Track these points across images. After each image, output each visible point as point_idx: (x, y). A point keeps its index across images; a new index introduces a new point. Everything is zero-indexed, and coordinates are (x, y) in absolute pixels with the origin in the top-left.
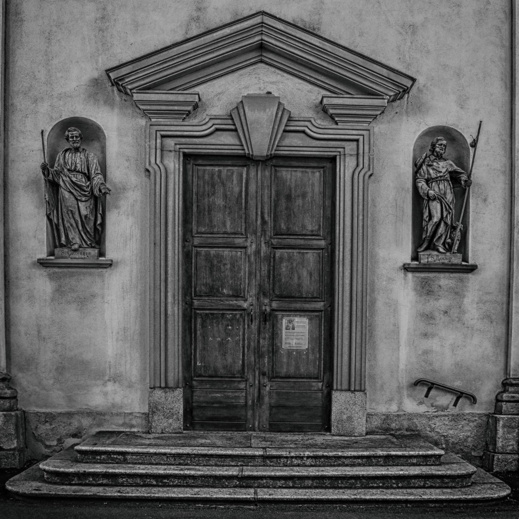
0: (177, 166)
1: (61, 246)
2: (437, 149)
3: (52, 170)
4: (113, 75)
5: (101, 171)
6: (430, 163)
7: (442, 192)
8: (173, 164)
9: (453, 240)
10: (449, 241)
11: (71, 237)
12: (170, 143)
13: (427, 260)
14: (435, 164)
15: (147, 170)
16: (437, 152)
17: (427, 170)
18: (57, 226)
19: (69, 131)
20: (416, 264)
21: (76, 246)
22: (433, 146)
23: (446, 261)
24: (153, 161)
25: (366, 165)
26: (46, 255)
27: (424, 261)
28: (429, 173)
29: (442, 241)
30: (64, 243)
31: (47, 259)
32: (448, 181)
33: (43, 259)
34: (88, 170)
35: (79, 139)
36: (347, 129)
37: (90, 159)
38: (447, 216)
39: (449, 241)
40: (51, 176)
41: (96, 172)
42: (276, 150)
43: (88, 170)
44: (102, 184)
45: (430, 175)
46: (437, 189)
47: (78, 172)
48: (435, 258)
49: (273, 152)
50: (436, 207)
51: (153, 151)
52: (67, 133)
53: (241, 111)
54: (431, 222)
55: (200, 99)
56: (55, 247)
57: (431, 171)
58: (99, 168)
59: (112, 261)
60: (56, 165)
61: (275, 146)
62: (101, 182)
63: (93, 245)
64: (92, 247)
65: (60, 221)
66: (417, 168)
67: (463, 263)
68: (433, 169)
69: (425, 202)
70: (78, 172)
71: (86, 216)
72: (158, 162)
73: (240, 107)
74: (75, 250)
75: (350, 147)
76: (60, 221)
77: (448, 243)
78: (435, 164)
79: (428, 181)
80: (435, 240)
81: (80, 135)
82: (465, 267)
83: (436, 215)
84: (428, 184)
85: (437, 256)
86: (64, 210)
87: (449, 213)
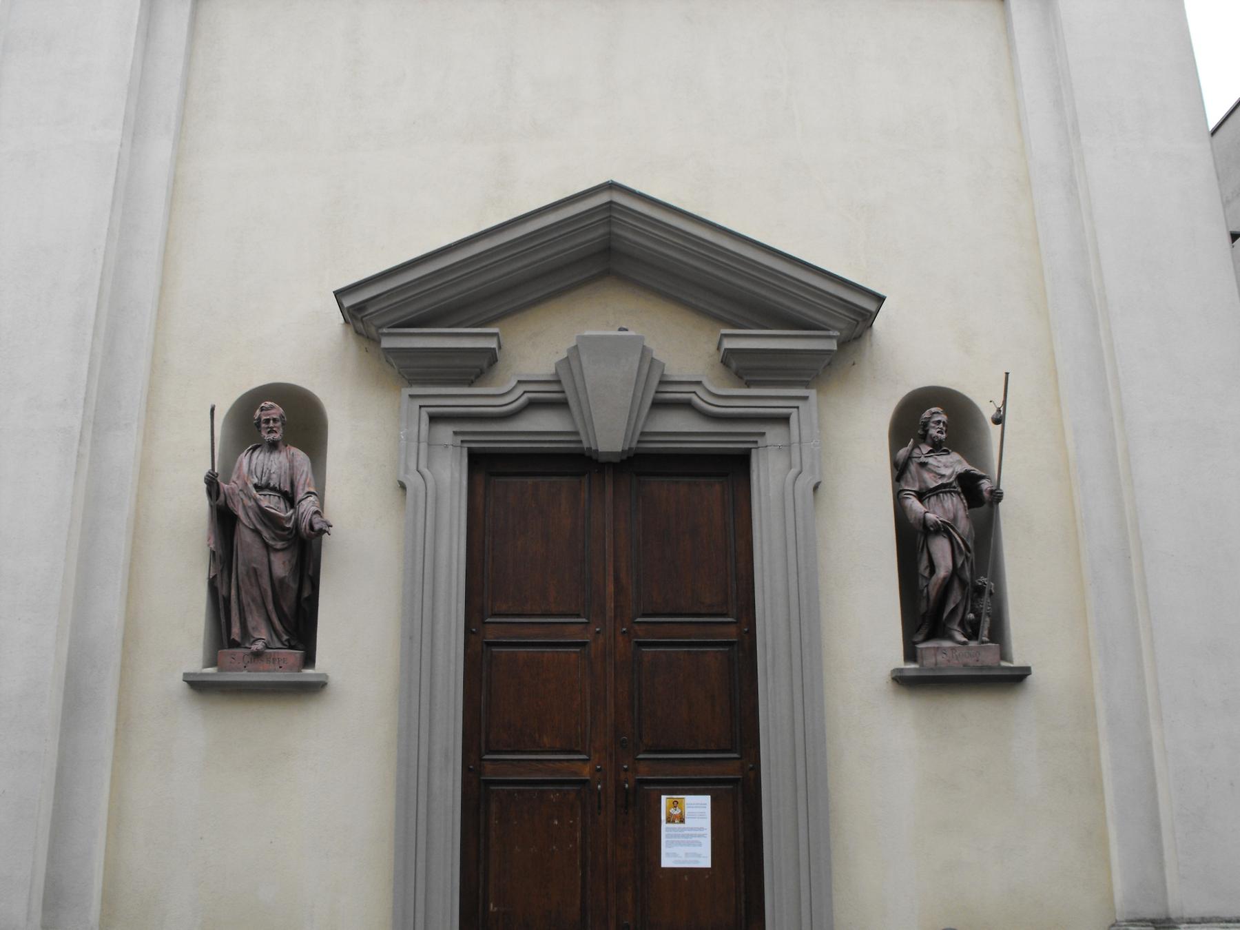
0: (457, 475)
1: (234, 644)
2: (933, 432)
3: (226, 486)
4: (349, 302)
5: (316, 488)
6: (923, 459)
7: (951, 516)
8: (451, 474)
9: (978, 615)
10: (972, 616)
11: (251, 623)
12: (445, 433)
13: (933, 660)
14: (930, 460)
15: (403, 487)
16: (933, 438)
17: (918, 473)
18: (227, 601)
19: (262, 409)
20: (915, 669)
21: (259, 646)
22: (925, 425)
23: (971, 662)
24: (413, 466)
25: (806, 467)
26: (201, 664)
27: (929, 661)
28: (922, 480)
29: (958, 619)
30: (237, 639)
31: (202, 674)
32: (959, 494)
33: (194, 674)
34: (292, 484)
35: (279, 424)
36: (765, 399)
37: (296, 464)
38: (963, 565)
39: (972, 616)
40: (222, 497)
41: (307, 490)
42: (639, 442)
43: (292, 484)
44: (317, 512)
45: (925, 482)
46: (939, 511)
47: (274, 489)
48: (949, 653)
49: (634, 445)
50: (941, 549)
51: (414, 444)
52: (258, 412)
53: (574, 364)
54: (934, 578)
55: (500, 347)
56: (223, 648)
57: (927, 476)
58: (312, 483)
59: (327, 677)
60: (234, 477)
61: (638, 433)
62: (314, 508)
63: (293, 643)
64: (291, 647)
65: (233, 592)
66: (900, 470)
67: (1004, 664)
68: (930, 471)
69: (920, 539)
70: (274, 489)
71: (282, 581)
72: (422, 467)
73: (571, 362)
74: (257, 655)
75: (773, 434)
76: (233, 592)
77: (970, 622)
78: (930, 460)
79: (921, 496)
80: (945, 615)
81: (282, 417)
82: (1008, 673)
83: (943, 563)
84: (921, 501)
85: (953, 649)
86: (241, 569)
87: (967, 557)
